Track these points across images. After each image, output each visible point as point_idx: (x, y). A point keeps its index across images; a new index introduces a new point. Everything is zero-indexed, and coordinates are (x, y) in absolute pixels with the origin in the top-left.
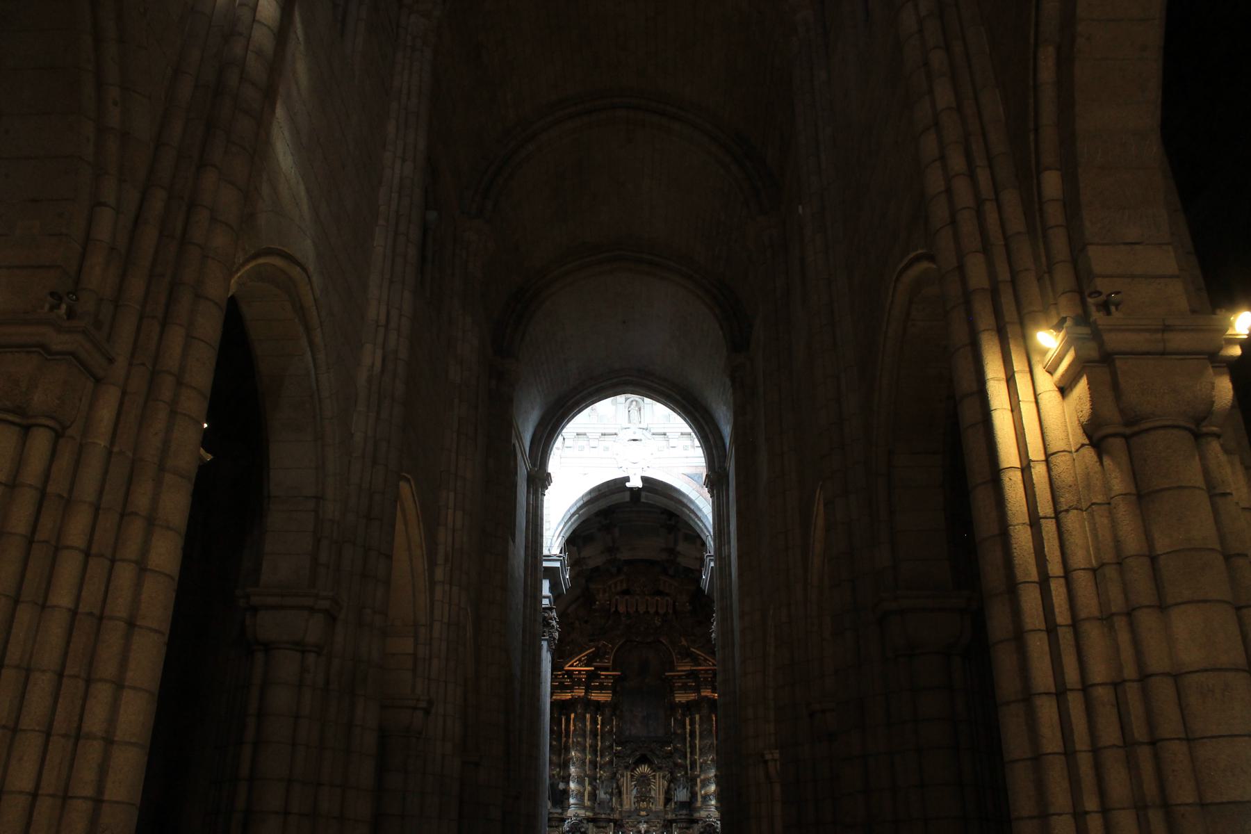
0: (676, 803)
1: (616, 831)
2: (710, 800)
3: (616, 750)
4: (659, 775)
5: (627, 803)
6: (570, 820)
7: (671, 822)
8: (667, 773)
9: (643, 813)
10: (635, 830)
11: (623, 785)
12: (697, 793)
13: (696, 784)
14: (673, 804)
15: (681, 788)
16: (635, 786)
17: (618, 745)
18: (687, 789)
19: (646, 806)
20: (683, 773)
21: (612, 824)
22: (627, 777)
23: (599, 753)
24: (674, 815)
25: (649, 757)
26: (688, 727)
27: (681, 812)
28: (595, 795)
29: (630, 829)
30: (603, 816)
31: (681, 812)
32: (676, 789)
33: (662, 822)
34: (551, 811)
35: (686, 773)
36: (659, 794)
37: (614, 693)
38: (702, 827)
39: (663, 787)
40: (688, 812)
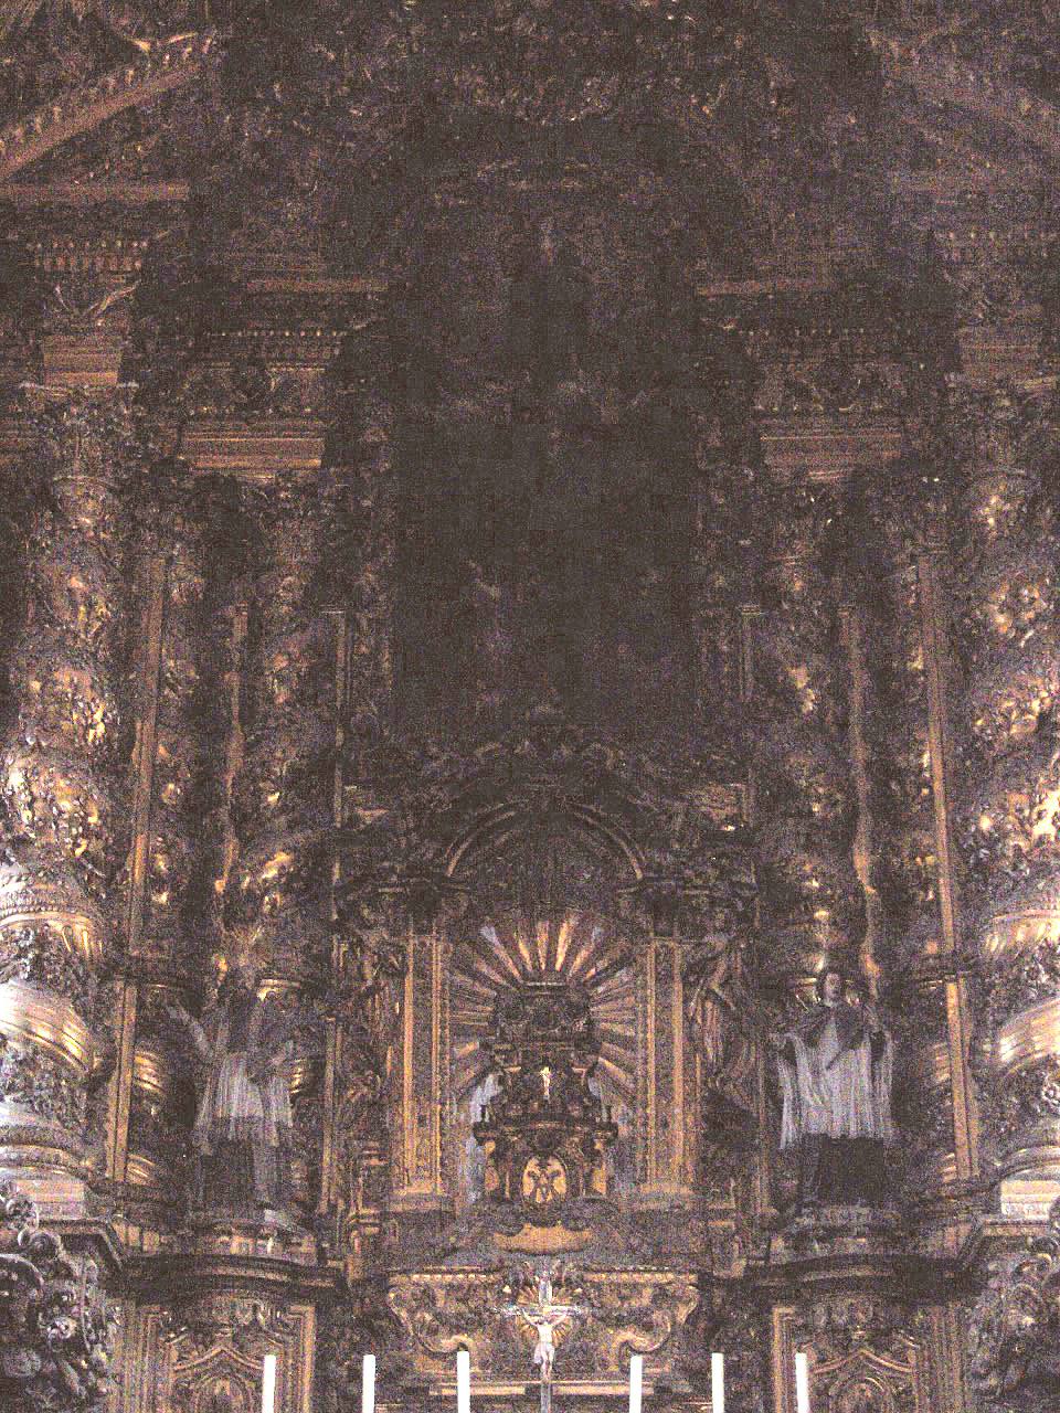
3: (354, 820)
8: (718, 941)
9: (533, 1236)
11: (396, 1031)
14: (760, 1184)
15: (830, 1040)
18: (877, 1052)
19: (560, 1185)
22: (422, 974)
23: (230, 849)
24: (778, 1244)
26: (861, 680)
27: (836, 1214)
29: (447, 1343)
30: (237, 1245)
36: (665, 1092)
37: (343, 449)
38: (1023, 1299)
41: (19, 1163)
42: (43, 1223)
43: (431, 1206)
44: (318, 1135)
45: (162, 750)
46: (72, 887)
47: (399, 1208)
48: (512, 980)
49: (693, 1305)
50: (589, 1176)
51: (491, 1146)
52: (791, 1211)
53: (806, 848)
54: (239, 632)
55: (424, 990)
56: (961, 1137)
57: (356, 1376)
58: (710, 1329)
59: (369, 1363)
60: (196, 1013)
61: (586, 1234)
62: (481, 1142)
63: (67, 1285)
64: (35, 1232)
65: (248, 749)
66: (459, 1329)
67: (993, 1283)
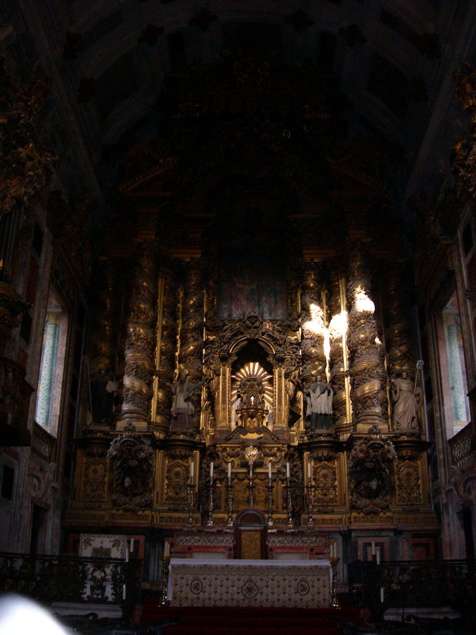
0: (308, 419)
1: (204, 466)
2: (373, 405)
3: (208, 339)
4: (280, 373)
5: (224, 418)
6: (119, 438)
7: (300, 449)
10: (237, 461)
11: (218, 389)
12: (345, 403)
13: (342, 387)
14: (302, 424)
15: (318, 391)
16: (239, 396)
17: (211, 331)
19: (256, 424)
20: (320, 368)
21: (198, 452)
22: (224, 375)
23: (179, 345)
24: (306, 438)
25: (262, 344)
27: (318, 431)
28: (170, 407)
30: (181, 437)
31: (318, 431)
32: (308, 395)
33: (285, 448)
34: (92, 428)
35: (324, 372)
38: (361, 451)
39: (287, 390)
40: (330, 431)
41: (132, 418)
42: (138, 432)
43: (226, 429)
44: (200, 412)
45: (164, 322)
46: (144, 354)
47: (219, 429)
48: (244, 376)
49: (286, 452)
50: (262, 422)
51: (240, 415)
52: (309, 430)
53: (312, 346)
54: (181, 294)
55: (224, 378)
56: (348, 413)
57: (209, 467)
58: (289, 457)
59: (212, 464)
60: (171, 383)
61: (262, 435)
62: (238, 414)
63: (143, 446)
64: (137, 434)
65: (183, 323)
66: (231, 457)
67: (355, 447)
